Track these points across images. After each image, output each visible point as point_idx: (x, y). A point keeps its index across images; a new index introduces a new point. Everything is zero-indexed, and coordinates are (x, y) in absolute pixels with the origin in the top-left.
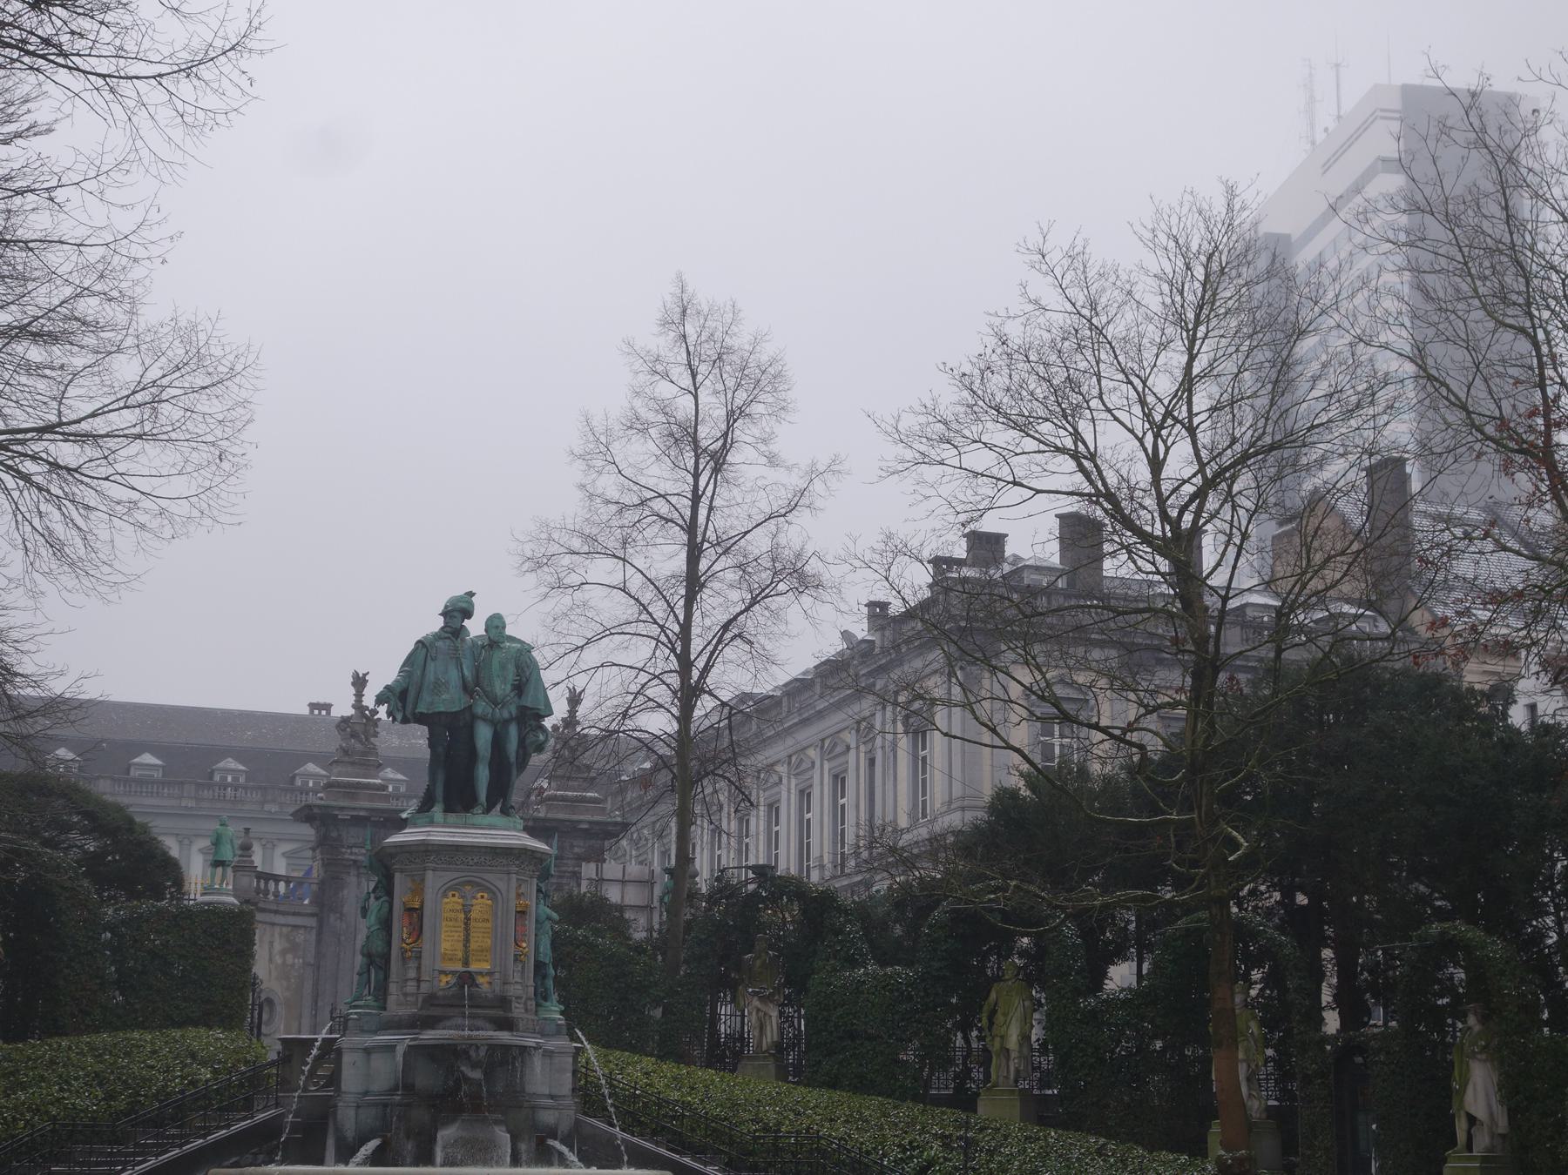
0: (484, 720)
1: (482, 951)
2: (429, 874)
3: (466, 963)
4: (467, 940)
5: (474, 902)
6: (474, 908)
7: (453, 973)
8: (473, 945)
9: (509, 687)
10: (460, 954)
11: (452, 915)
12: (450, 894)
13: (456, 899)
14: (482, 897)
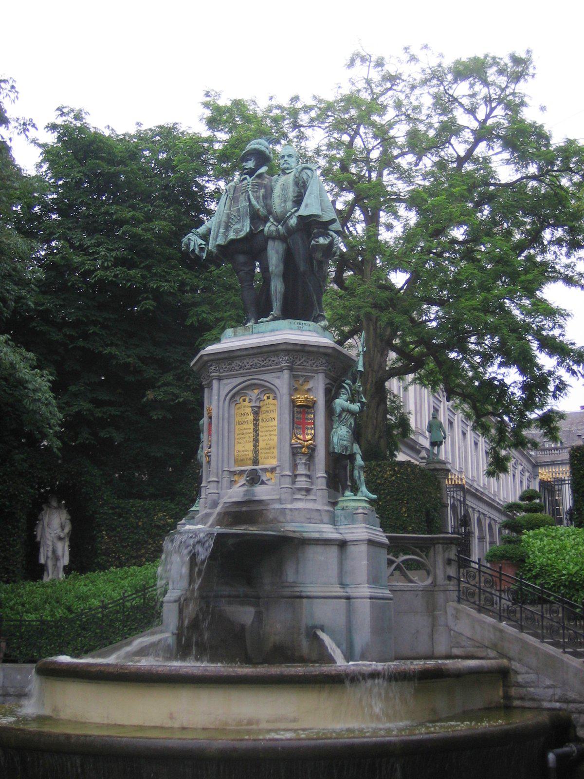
0: (274, 239)
1: (270, 448)
2: (215, 383)
3: (256, 462)
4: (256, 440)
5: (262, 404)
6: (263, 409)
7: (242, 473)
8: (262, 444)
9: (289, 204)
10: (250, 454)
11: (244, 418)
12: (241, 400)
13: (246, 403)
14: (268, 398)
